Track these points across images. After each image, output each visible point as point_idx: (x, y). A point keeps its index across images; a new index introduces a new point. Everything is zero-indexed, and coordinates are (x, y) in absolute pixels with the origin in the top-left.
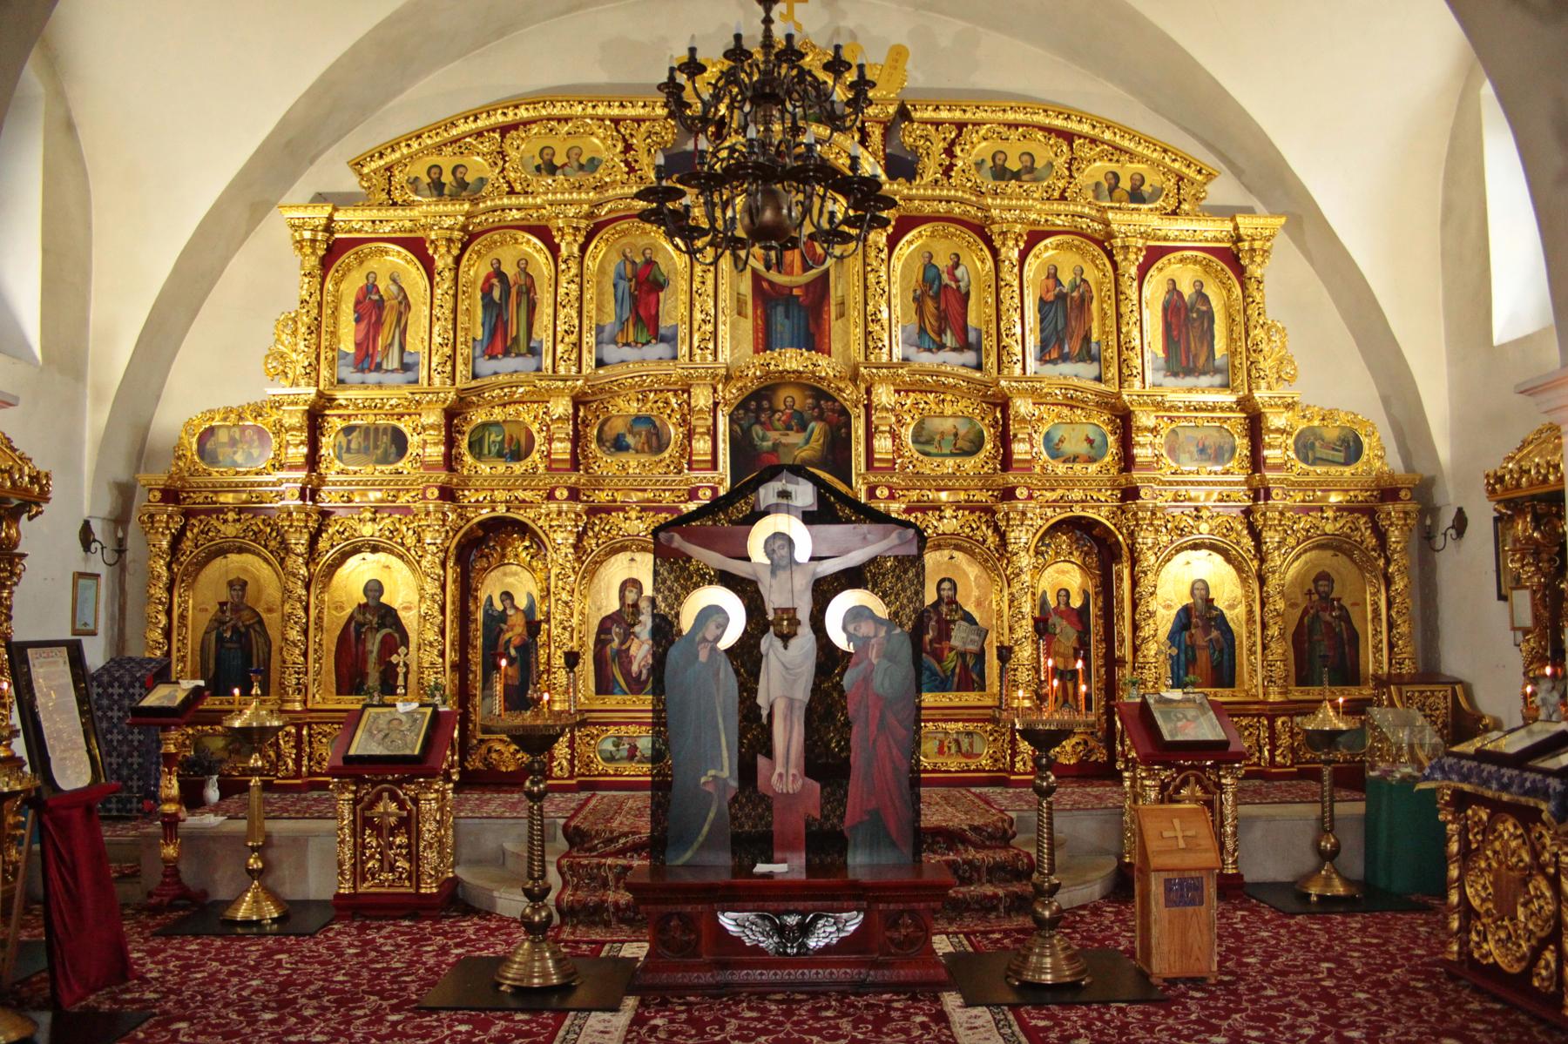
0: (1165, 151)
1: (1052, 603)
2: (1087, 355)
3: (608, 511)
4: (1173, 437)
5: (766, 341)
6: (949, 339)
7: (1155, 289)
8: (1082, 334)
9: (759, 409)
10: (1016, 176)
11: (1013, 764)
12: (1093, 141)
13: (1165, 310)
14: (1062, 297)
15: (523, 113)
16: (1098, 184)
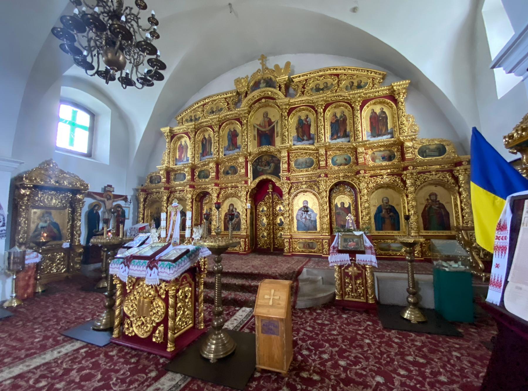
0: (368, 71)
1: (339, 206)
2: (346, 135)
3: (225, 188)
4: (373, 155)
5: (260, 144)
6: (305, 138)
7: (366, 112)
8: (344, 130)
9: (259, 161)
10: (322, 89)
11: (323, 252)
12: (345, 74)
13: (370, 119)
14: (337, 121)
15: (207, 101)
16: (347, 86)
